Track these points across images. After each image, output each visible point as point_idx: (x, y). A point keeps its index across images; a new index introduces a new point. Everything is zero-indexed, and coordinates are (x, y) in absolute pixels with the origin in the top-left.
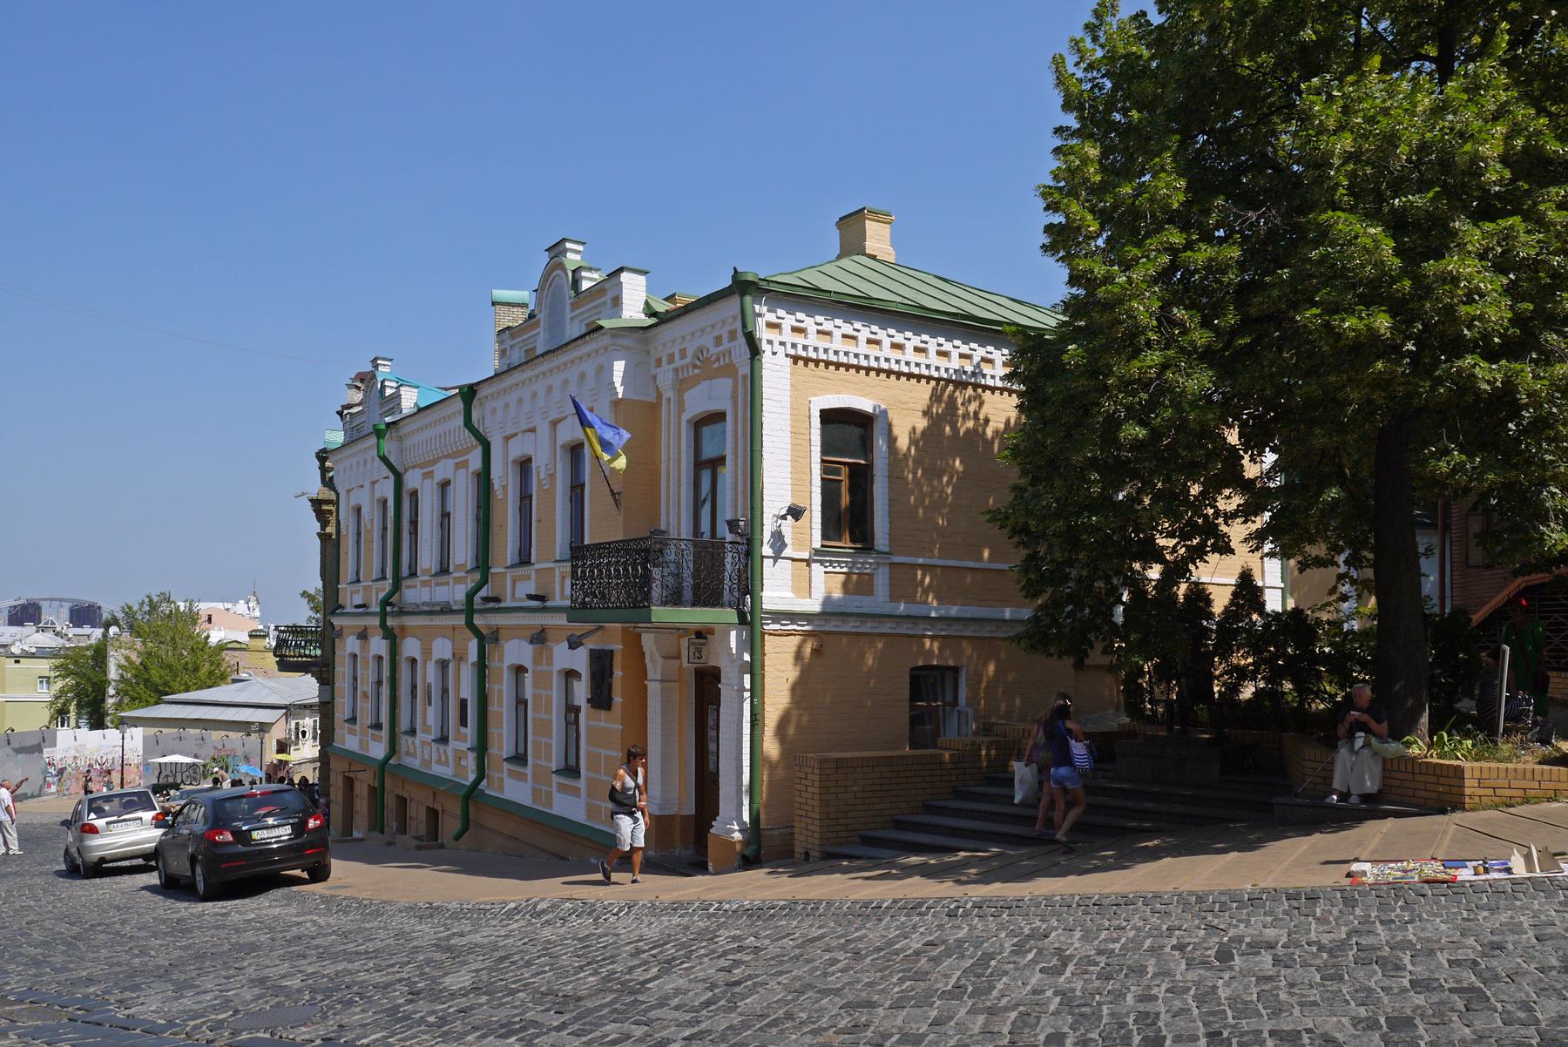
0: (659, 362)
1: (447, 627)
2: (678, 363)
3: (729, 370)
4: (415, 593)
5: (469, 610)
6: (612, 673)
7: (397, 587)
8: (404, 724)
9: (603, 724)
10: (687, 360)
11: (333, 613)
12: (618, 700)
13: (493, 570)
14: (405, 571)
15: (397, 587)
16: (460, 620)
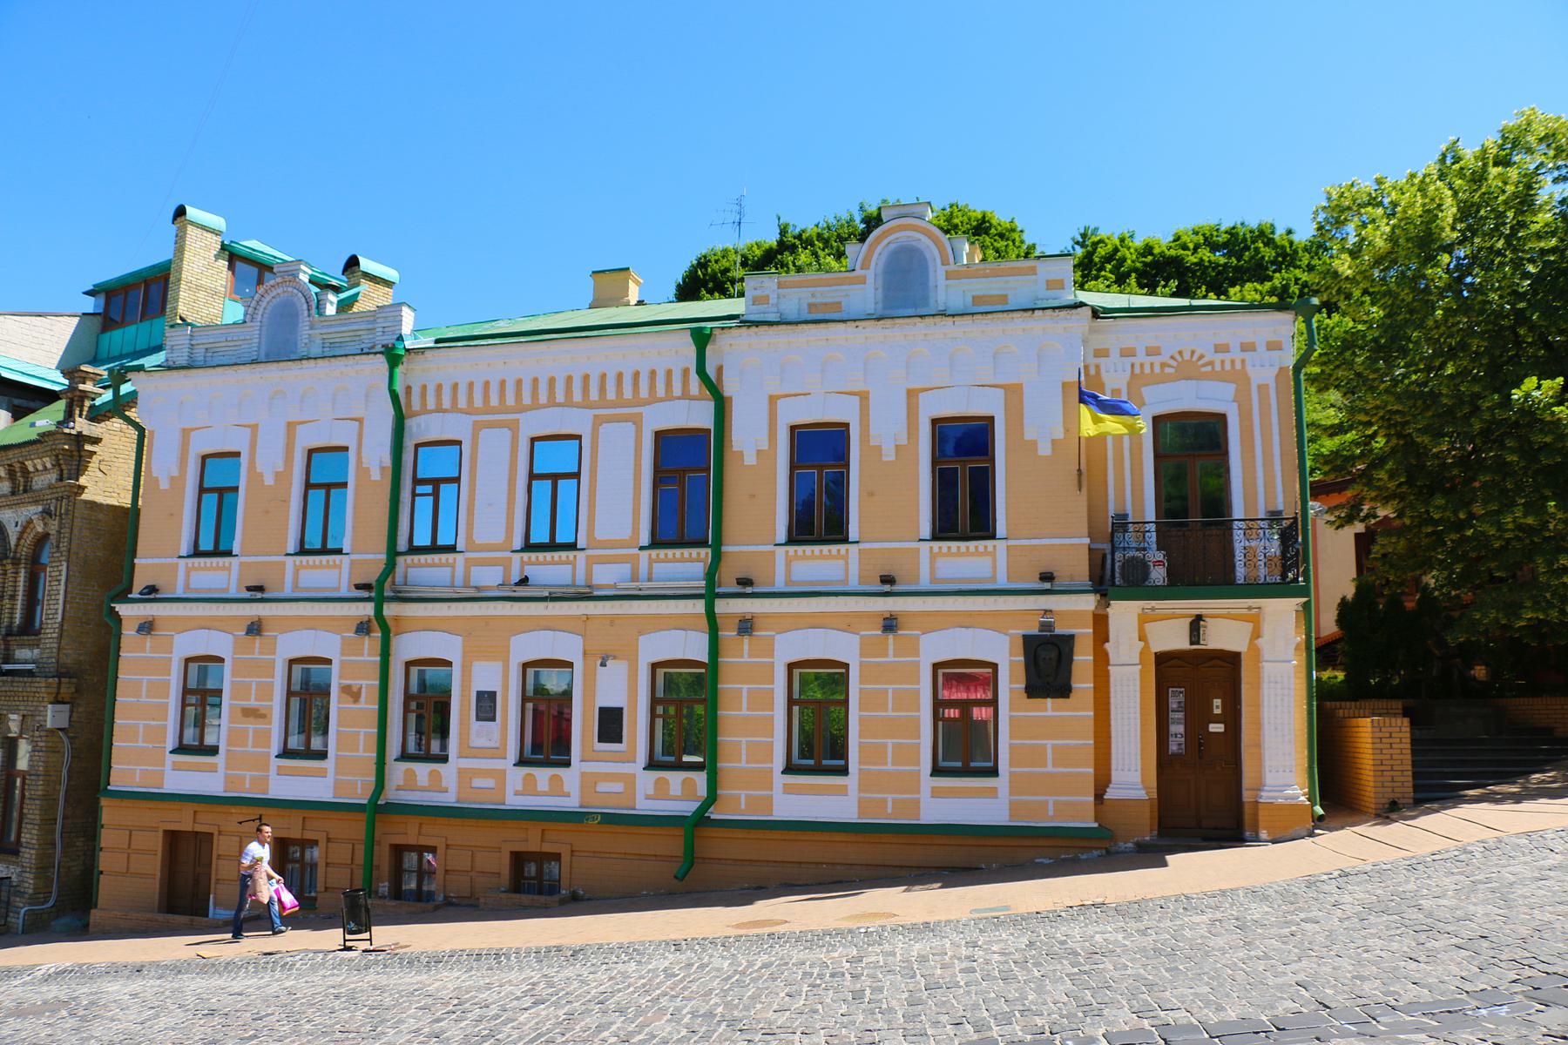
0: (1101, 353)
1: (578, 617)
2: (1141, 357)
3: (1239, 378)
4: (422, 572)
5: (711, 595)
6: (1071, 660)
7: (391, 566)
8: (394, 748)
9: (1050, 713)
10: (1165, 358)
11: (123, 596)
12: (1082, 682)
13: (724, 549)
14: (402, 545)
15: (391, 566)
16: (699, 607)
